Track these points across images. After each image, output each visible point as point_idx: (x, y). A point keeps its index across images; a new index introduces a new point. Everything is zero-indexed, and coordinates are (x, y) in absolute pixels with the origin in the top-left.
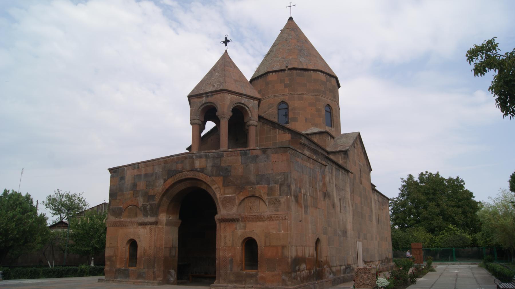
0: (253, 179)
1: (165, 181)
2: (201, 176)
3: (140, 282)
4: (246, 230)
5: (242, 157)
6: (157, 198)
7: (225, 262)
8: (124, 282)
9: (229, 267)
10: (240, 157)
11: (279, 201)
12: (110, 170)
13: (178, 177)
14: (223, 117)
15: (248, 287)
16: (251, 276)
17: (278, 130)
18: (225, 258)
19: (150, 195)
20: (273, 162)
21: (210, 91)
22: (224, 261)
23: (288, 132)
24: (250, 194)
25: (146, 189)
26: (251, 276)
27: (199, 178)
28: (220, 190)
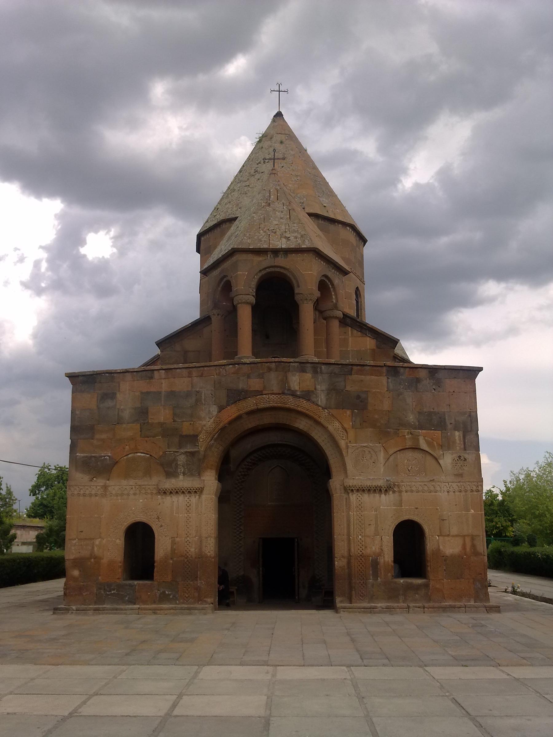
0: (411, 418)
1: (221, 409)
2: (303, 405)
3: (170, 610)
4: (403, 507)
5: (388, 378)
6: (201, 440)
7: (361, 564)
8: (128, 612)
9: (371, 572)
10: (386, 377)
11: (465, 460)
12: (72, 377)
13: (250, 404)
14: (310, 298)
15: (416, 607)
16: (417, 588)
17: (350, 328)
18: (361, 557)
19: (184, 434)
20: (450, 392)
21: (291, 247)
22: (359, 561)
23: (370, 335)
24: (409, 444)
25: (174, 421)
26: (417, 588)
27: (299, 409)
28: (346, 434)
